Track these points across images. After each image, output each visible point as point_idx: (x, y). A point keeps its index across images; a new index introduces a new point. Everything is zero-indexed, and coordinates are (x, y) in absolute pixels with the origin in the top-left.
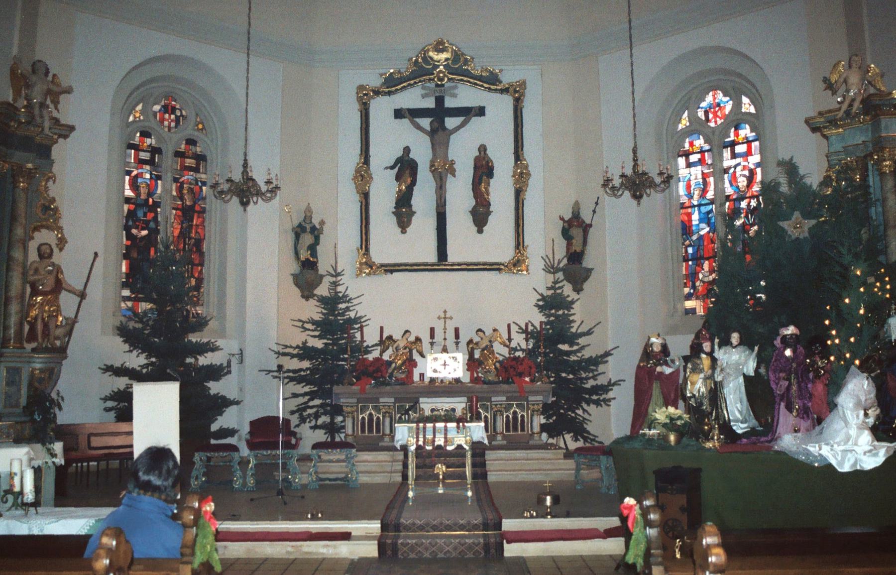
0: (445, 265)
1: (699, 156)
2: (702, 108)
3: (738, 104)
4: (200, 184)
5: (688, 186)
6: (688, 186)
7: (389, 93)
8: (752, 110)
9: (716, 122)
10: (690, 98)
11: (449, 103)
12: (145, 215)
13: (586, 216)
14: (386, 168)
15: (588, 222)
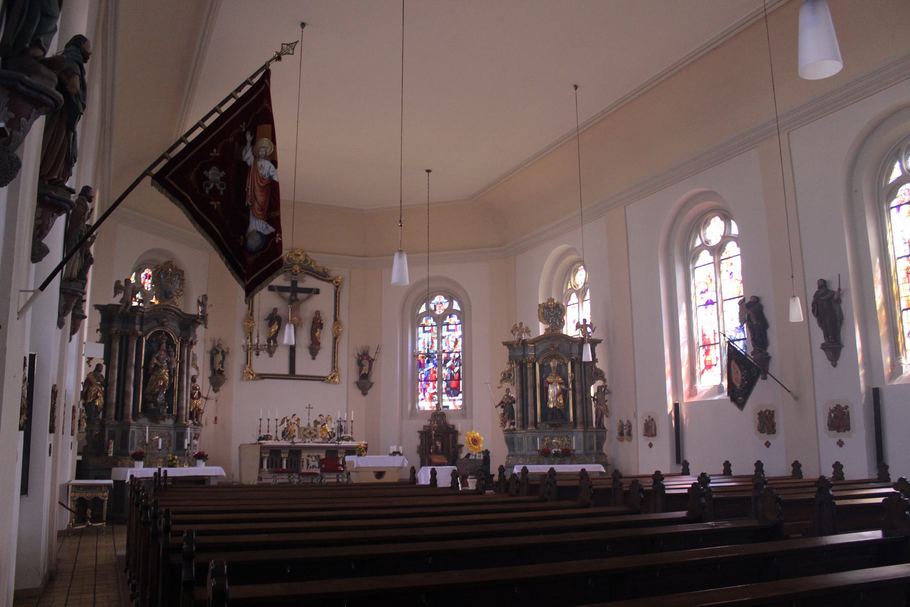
0: (295, 376)
1: (430, 328)
3: (451, 305)
5: (424, 343)
8: (459, 309)
9: (440, 312)
11: (300, 285)
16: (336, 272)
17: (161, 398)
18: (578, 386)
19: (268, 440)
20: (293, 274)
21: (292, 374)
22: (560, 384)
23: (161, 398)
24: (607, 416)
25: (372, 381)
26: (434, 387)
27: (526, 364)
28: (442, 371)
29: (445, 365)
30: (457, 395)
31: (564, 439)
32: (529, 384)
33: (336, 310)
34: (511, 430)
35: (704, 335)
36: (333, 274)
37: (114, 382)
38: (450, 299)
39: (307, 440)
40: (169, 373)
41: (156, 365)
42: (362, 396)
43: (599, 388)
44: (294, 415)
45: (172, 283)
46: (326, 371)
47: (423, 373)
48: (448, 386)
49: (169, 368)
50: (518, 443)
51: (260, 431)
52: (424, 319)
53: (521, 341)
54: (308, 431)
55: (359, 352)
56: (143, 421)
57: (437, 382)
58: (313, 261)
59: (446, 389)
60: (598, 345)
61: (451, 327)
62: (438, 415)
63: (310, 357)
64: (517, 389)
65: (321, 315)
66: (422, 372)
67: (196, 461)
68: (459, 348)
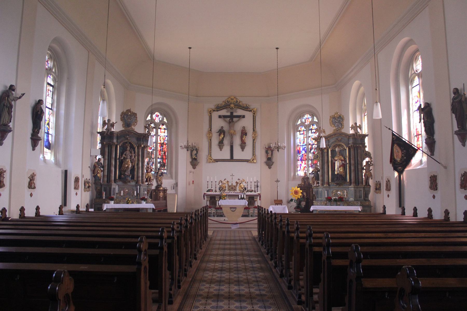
1: (302, 132)
3: (313, 119)
4: (165, 136)
5: (300, 140)
6: (300, 140)
7: (217, 111)
8: (317, 121)
16: (253, 106)
17: (128, 173)
18: (352, 162)
19: (211, 192)
20: (231, 109)
21: (232, 159)
22: (342, 160)
23: (128, 173)
24: (372, 179)
25: (273, 161)
26: (305, 164)
27: (324, 150)
28: (309, 155)
29: (310, 152)
32: (325, 161)
33: (254, 125)
34: (318, 186)
35: (417, 129)
36: (252, 107)
37: (106, 166)
38: (312, 116)
39: (231, 192)
40: (131, 161)
41: (124, 158)
44: (225, 179)
45: (130, 120)
46: (249, 157)
47: (300, 156)
49: (131, 159)
50: (320, 193)
51: (208, 187)
52: (300, 127)
54: (231, 187)
55: (266, 147)
56: (120, 183)
61: (313, 131)
63: (241, 150)
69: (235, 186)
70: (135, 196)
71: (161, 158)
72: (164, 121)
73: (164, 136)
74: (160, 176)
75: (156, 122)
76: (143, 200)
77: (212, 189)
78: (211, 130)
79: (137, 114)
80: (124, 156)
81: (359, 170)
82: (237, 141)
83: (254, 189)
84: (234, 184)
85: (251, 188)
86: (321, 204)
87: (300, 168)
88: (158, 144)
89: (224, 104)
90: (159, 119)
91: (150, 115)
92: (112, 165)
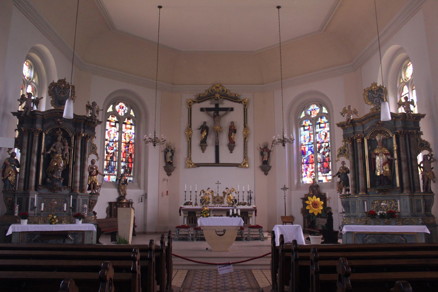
0: (219, 164)
1: (308, 127)
2: (309, 110)
3: (321, 110)
4: (132, 134)
5: (304, 138)
7: (199, 102)
8: (326, 112)
9: (314, 116)
10: (305, 107)
11: (221, 106)
12: (113, 145)
13: (269, 148)
14: (197, 129)
15: (270, 149)
16: (244, 96)
18: (403, 156)
19: (189, 205)
20: (216, 100)
21: (217, 163)
22: (386, 154)
23: (58, 175)
24: (434, 182)
25: (271, 165)
26: (312, 168)
27: (356, 140)
28: (317, 156)
29: (319, 152)
30: (328, 172)
31: (392, 202)
32: (359, 156)
33: (245, 120)
34: (347, 195)
36: (242, 98)
39: (216, 205)
40: (62, 157)
41: (52, 152)
42: (265, 175)
43: (425, 157)
44: (209, 188)
45: (64, 94)
47: (305, 159)
48: (323, 166)
49: (62, 154)
51: (185, 199)
52: (304, 121)
53: (349, 121)
54: (217, 199)
56: (44, 191)
57: (314, 164)
58: (228, 90)
59: (320, 168)
60: (422, 119)
61: (322, 125)
62: (314, 187)
63: (229, 151)
64: (350, 161)
65: (234, 124)
66: (304, 158)
67: (75, 220)
68: (328, 139)
69: (221, 198)
70: (65, 211)
71: (125, 162)
72: (131, 114)
73: (131, 133)
74: (123, 184)
75: (120, 115)
76: (77, 218)
77: (191, 201)
78: (190, 127)
79: (75, 87)
80: (52, 149)
81: (414, 168)
82: (224, 140)
83: (247, 202)
84: (221, 195)
85: (243, 200)
86: (356, 223)
87: (306, 173)
88: (123, 144)
89: (207, 94)
90: (124, 111)
91: (111, 106)
92: (33, 163)
